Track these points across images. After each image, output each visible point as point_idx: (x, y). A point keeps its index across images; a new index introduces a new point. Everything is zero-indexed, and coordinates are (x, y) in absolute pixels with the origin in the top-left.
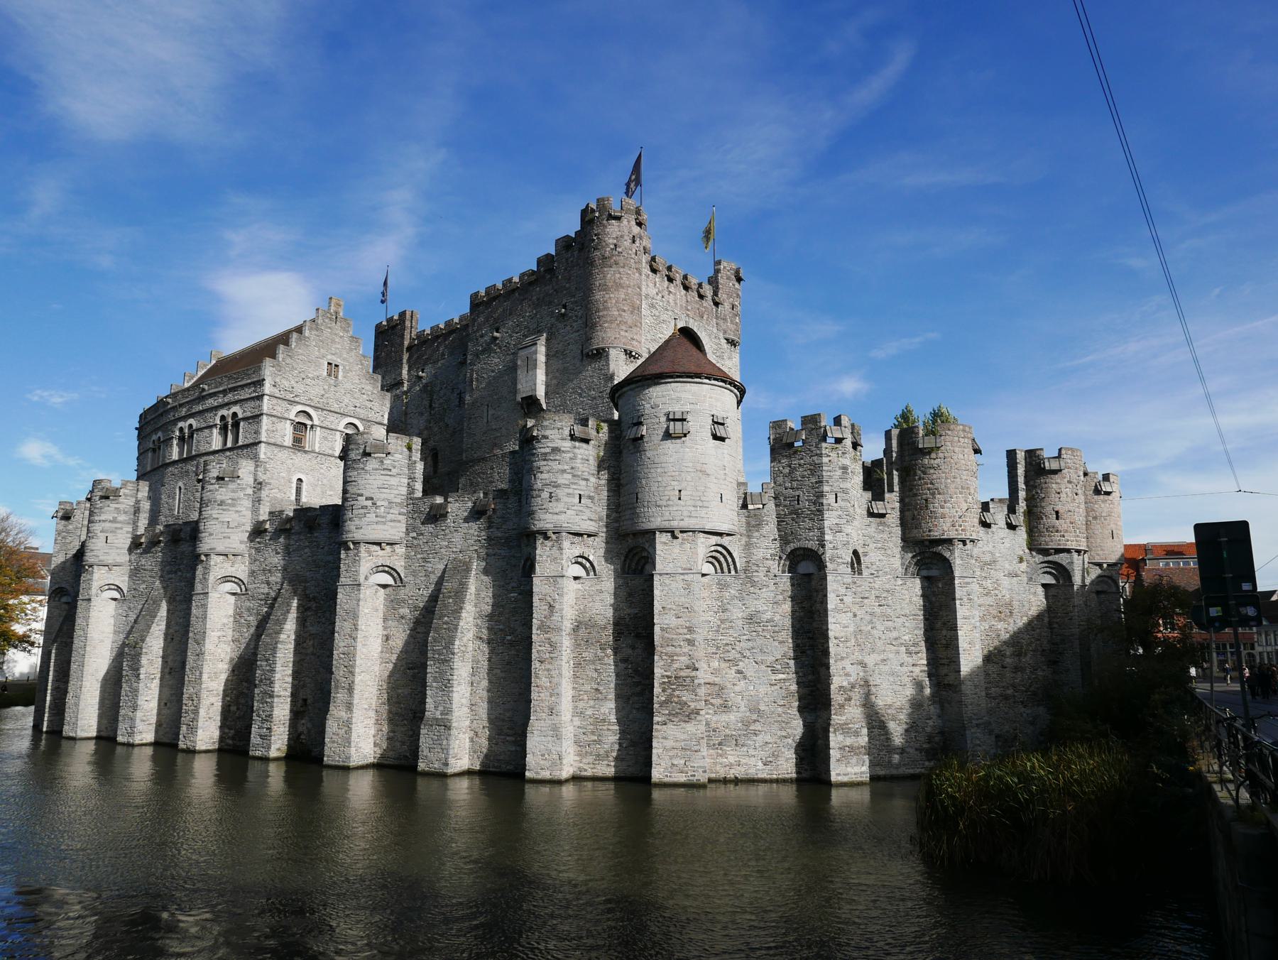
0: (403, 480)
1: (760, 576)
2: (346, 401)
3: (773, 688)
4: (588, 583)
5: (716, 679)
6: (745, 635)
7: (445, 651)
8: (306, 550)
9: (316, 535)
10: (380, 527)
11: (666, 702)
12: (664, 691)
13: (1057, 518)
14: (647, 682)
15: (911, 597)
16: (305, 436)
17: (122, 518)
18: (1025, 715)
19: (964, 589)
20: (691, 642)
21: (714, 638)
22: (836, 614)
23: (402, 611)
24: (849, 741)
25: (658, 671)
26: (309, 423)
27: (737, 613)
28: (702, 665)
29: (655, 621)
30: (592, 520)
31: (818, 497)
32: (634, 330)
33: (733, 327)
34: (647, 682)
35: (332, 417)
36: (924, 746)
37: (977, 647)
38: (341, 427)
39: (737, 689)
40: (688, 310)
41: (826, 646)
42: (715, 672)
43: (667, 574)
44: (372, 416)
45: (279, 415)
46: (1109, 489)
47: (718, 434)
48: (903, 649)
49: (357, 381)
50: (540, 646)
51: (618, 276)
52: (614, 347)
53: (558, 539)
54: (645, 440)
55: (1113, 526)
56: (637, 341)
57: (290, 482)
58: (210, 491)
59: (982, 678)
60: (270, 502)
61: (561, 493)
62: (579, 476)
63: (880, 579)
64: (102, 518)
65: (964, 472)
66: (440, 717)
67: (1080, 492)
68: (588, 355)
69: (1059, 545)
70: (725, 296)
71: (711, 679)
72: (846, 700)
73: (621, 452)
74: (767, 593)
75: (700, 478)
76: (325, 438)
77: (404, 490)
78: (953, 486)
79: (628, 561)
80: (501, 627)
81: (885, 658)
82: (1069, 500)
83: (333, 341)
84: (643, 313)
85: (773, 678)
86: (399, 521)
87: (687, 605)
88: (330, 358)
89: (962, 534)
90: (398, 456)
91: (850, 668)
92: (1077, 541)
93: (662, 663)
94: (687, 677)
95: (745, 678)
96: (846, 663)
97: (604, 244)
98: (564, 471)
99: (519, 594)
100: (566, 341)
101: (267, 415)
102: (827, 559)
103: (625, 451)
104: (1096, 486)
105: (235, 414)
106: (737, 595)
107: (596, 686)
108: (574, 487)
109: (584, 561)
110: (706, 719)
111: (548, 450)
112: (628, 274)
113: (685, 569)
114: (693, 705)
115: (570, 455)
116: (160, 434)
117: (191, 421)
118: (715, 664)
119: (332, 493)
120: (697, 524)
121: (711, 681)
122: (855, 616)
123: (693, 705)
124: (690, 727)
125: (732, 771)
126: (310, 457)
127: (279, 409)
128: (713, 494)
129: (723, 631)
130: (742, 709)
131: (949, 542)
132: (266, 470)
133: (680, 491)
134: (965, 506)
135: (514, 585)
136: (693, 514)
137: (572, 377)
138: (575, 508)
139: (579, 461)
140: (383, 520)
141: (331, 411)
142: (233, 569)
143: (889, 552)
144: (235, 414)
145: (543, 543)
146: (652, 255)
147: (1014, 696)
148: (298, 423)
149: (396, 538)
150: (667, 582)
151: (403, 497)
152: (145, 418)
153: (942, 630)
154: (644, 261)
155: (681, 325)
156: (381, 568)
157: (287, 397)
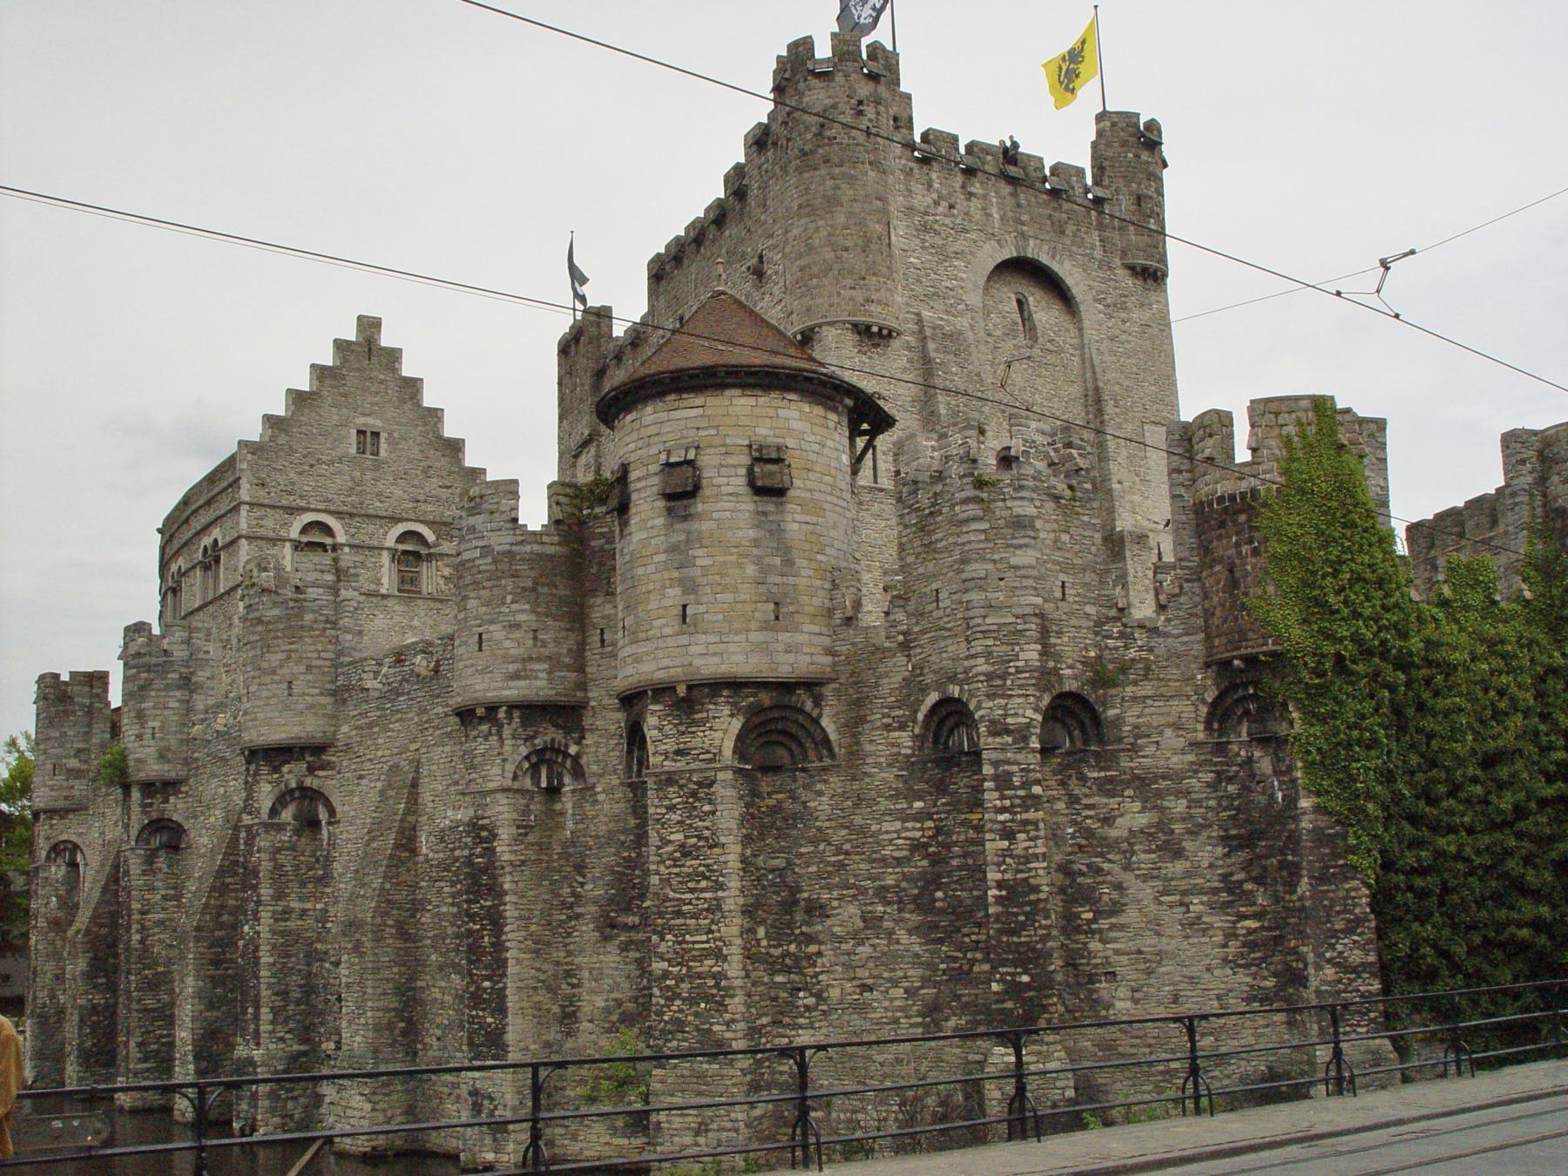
2: (398, 492)
26: (328, 541)
32: (872, 281)
38: (390, 541)
40: (1022, 224)
45: (271, 534)
49: (420, 457)
51: (829, 183)
56: (879, 303)
70: (1120, 183)
88: (361, 421)
105: (216, 541)
136: (712, 648)
141: (368, 516)
144: (216, 541)
155: (1008, 253)
157: (285, 502)
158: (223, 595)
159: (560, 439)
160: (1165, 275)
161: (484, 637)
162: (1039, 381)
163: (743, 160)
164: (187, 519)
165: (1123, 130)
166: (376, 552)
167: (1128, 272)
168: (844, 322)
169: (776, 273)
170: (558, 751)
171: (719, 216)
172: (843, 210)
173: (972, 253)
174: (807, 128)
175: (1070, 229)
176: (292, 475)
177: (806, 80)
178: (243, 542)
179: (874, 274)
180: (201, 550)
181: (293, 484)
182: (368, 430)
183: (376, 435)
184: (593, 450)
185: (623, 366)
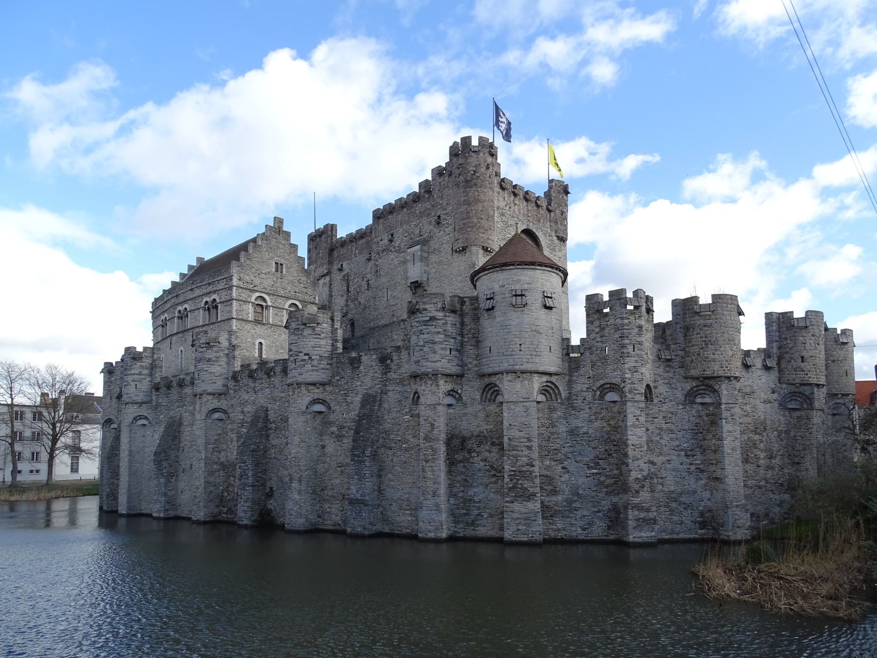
0: (329, 341)
1: (578, 403)
4: (458, 409)
5: (548, 473)
6: (568, 443)
7: (361, 455)
8: (267, 390)
9: (272, 379)
10: (315, 373)
11: (514, 487)
12: (511, 480)
14: (500, 474)
15: (689, 417)
16: (262, 313)
18: (773, 499)
20: (529, 448)
21: (546, 445)
22: (633, 429)
23: (332, 429)
24: (642, 515)
25: (507, 467)
26: (264, 304)
27: (562, 428)
28: (537, 463)
29: (504, 434)
30: (458, 366)
32: (489, 232)
33: (562, 228)
34: (500, 474)
35: (280, 300)
36: (698, 519)
38: (286, 307)
40: (529, 216)
41: (626, 451)
42: (548, 468)
43: (512, 402)
44: (307, 298)
45: (244, 300)
46: (845, 341)
47: (548, 305)
48: (683, 453)
49: (296, 275)
52: (475, 245)
53: (436, 379)
54: (495, 310)
55: (847, 367)
57: (254, 344)
58: (201, 352)
59: (741, 473)
60: (241, 358)
61: (437, 347)
62: (449, 335)
67: (821, 342)
68: (456, 252)
71: (545, 473)
72: (640, 487)
73: (479, 319)
74: (584, 415)
75: (534, 336)
76: (276, 314)
77: (329, 348)
78: (722, 339)
79: (485, 393)
80: (399, 438)
81: (670, 459)
82: (812, 348)
83: (278, 248)
84: (495, 220)
85: (588, 472)
86: (328, 369)
87: (527, 423)
90: (325, 325)
92: (818, 378)
94: (527, 471)
95: (568, 472)
96: (641, 463)
97: (466, 171)
98: (439, 333)
99: (411, 417)
100: (441, 242)
101: (236, 300)
103: (481, 318)
104: (835, 338)
105: (214, 300)
106: (562, 415)
108: (447, 343)
109: (454, 394)
110: (541, 499)
111: (428, 318)
112: (484, 192)
113: (524, 398)
114: (531, 490)
115: (442, 321)
116: (166, 315)
117: (186, 306)
118: (548, 463)
119: (282, 351)
120: (533, 367)
121: (544, 474)
122: (647, 430)
123: (531, 490)
124: (530, 505)
125: (560, 534)
126: (266, 327)
127: (244, 295)
128: (544, 347)
129: (553, 441)
132: (237, 337)
133: (520, 345)
135: (407, 410)
137: (445, 267)
138: (447, 358)
139: (449, 325)
140: (317, 368)
141: (279, 296)
142: (219, 404)
144: (214, 300)
145: (425, 382)
147: (766, 487)
148: (257, 305)
150: (512, 407)
151: (330, 353)
152: (156, 305)
153: (711, 440)
154: (496, 182)
155: (524, 227)
156: (317, 401)
158: (221, 321)
160: (566, 239)
163: (430, 179)
164: (192, 290)
165: (559, 187)
166: (282, 310)
169: (448, 224)
170: (455, 392)
171: (415, 198)
174: (469, 172)
176: (252, 277)
177: (469, 153)
178: (234, 301)
179: (490, 229)
184: (328, 278)
185: (345, 248)
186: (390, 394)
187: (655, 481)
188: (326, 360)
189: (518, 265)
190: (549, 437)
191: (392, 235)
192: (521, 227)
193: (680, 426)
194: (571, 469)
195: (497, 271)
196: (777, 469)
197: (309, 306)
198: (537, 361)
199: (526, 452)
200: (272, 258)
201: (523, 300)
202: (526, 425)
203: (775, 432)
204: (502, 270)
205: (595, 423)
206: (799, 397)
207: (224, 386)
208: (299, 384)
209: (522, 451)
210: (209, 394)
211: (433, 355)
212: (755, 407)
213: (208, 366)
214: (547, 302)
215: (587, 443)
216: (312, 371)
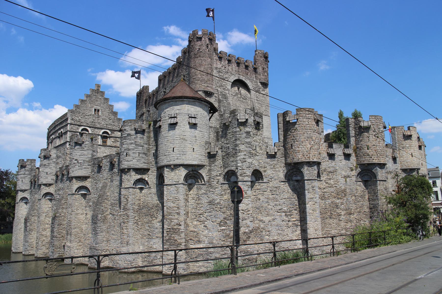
0: (89, 152)
2: (103, 123)
3: (219, 233)
5: (195, 229)
6: (208, 210)
7: (96, 219)
12: (168, 235)
13: (368, 149)
17: (27, 173)
19: (311, 185)
20: (178, 214)
27: (205, 200)
28: (182, 223)
29: (164, 205)
31: (236, 146)
33: (264, 77)
35: (96, 130)
37: (318, 212)
39: (204, 233)
40: (239, 72)
42: (195, 226)
50: (123, 216)
51: (200, 61)
54: (162, 127)
59: (320, 226)
61: (130, 153)
62: (138, 145)
63: (272, 182)
64: (21, 173)
65: (309, 131)
66: (95, 245)
69: (369, 161)
70: (259, 65)
72: (247, 238)
77: (90, 156)
83: (97, 101)
86: (88, 168)
87: (178, 198)
88: (95, 107)
89: (308, 159)
90: (87, 143)
91: (249, 223)
93: (167, 223)
96: (248, 222)
98: (132, 143)
101: (69, 131)
102: (239, 175)
105: (62, 132)
107: (149, 233)
111: (126, 135)
112: (205, 60)
113: (176, 182)
118: (195, 223)
127: (74, 128)
129: (199, 209)
130: (206, 242)
131: (302, 164)
133: (173, 148)
134: (309, 146)
136: (179, 158)
138: (137, 158)
139: (138, 138)
140: (81, 168)
143: (277, 170)
144: (62, 132)
146: (219, 50)
149: (87, 175)
150: (169, 187)
153: (302, 204)
155: (236, 78)
159: (137, 114)
161: (127, 153)
162: (242, 105)
167: (260, 84)
168: (202, 91)
170: (143, 179)
172: (203, 67)
173: (229, 78)
175: (249, 74)
180: (58, 134)
181: (80, 120)
182: (97, 109)
183: (98, 110)
186: (114, 182)
187: (264, 233)
188: (87, 163)
189: (172, 99)
190: (197, 207)
191: (166, 89)
192: (233, 78)
193: (282, 196)
194: (209, 227)
195: (163, 104)
196: (355, 221)
197: (115, 132)
198: (184, 158)
199: (177, 216)
200: (93, 107)
201: (175, 120)
202: (177, 199)
203: (353, 197)
204: (165, 103)
205: (225, 197)
206: (369, 173)
207: (52, 179)
208: (72, 178)
209: (174, 216)
210: (44, 185)
211: (128, 157)
212: (337, 181)
213: (44, 168)
214: (190, 120)
215: (220, 209)
216: (79, 169)
